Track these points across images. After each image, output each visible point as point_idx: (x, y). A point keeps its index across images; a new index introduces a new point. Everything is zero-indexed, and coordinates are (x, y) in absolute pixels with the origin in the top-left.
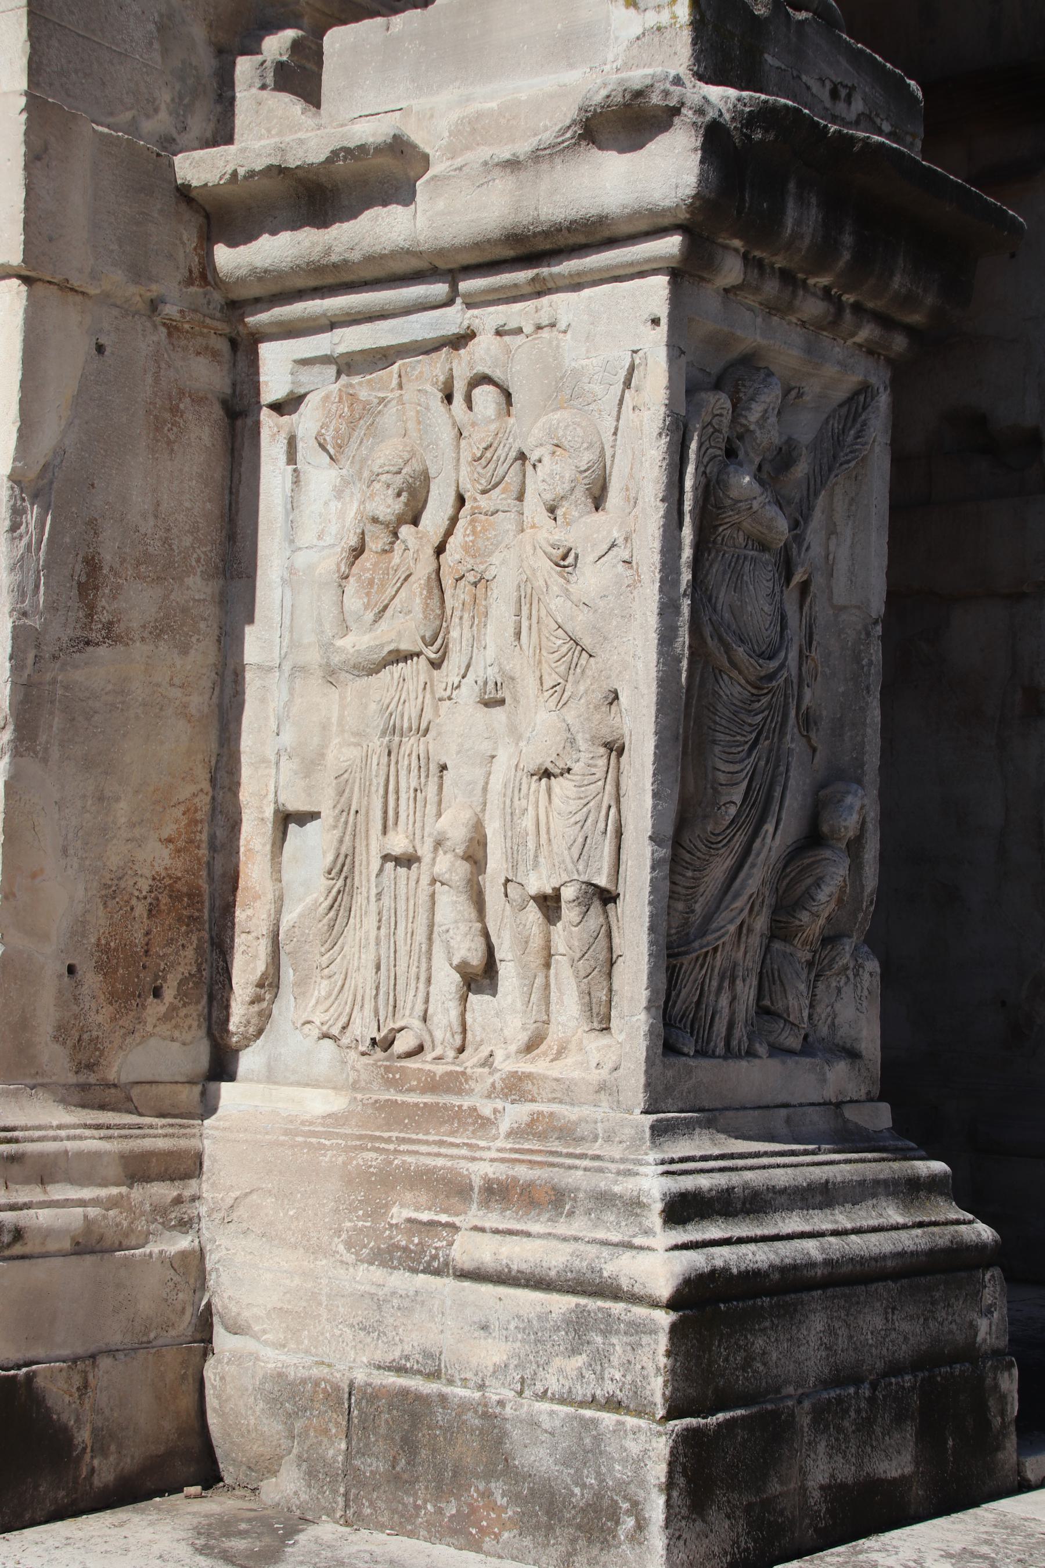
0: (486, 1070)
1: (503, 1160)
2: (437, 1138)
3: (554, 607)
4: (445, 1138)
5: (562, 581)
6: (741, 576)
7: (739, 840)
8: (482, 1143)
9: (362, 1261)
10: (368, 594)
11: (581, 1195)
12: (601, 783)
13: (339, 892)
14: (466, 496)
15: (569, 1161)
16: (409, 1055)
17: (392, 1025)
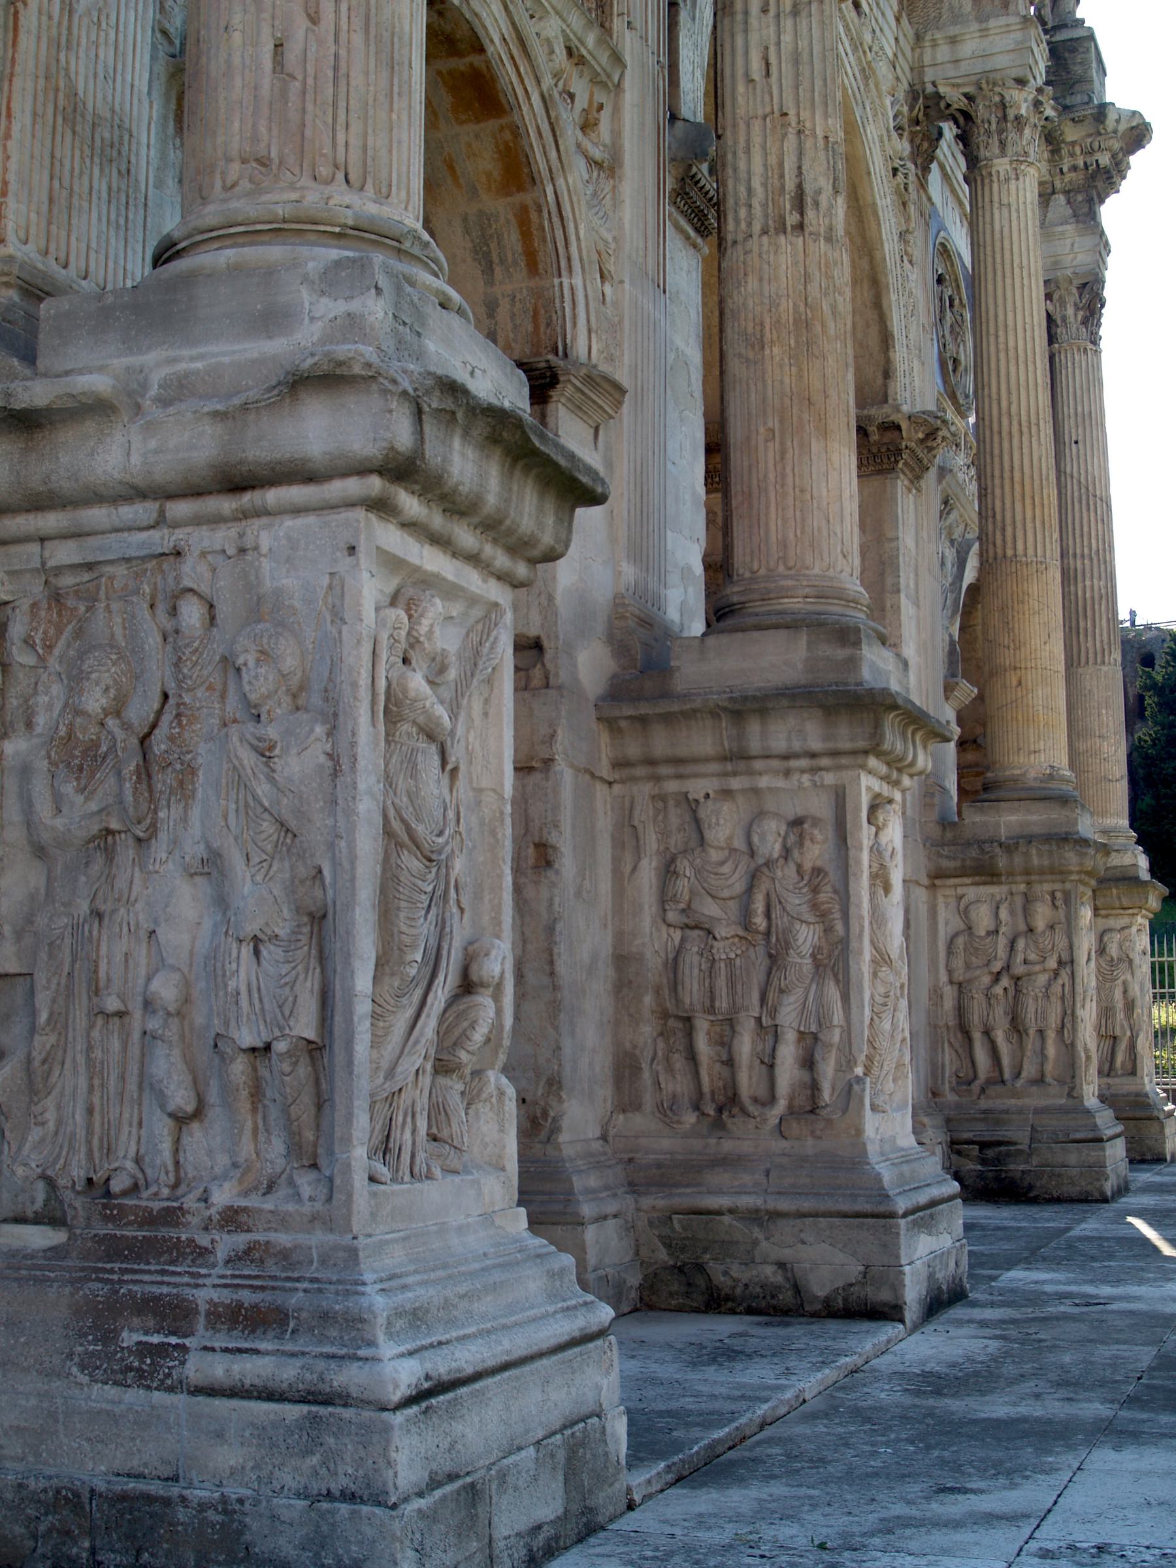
0: (203, 1205)
1: (225, 1286)
2: (159, 1268)
3: (260, 793)
5: (266, 770)
6: (415, 765)
7: (419, 993)
8: (203, 1271)
9: (96, 1381)
10: (78, 779)
11: (304, 1315)
14: (170, 693)
15: (288, 1285)
16: (125, 1193)
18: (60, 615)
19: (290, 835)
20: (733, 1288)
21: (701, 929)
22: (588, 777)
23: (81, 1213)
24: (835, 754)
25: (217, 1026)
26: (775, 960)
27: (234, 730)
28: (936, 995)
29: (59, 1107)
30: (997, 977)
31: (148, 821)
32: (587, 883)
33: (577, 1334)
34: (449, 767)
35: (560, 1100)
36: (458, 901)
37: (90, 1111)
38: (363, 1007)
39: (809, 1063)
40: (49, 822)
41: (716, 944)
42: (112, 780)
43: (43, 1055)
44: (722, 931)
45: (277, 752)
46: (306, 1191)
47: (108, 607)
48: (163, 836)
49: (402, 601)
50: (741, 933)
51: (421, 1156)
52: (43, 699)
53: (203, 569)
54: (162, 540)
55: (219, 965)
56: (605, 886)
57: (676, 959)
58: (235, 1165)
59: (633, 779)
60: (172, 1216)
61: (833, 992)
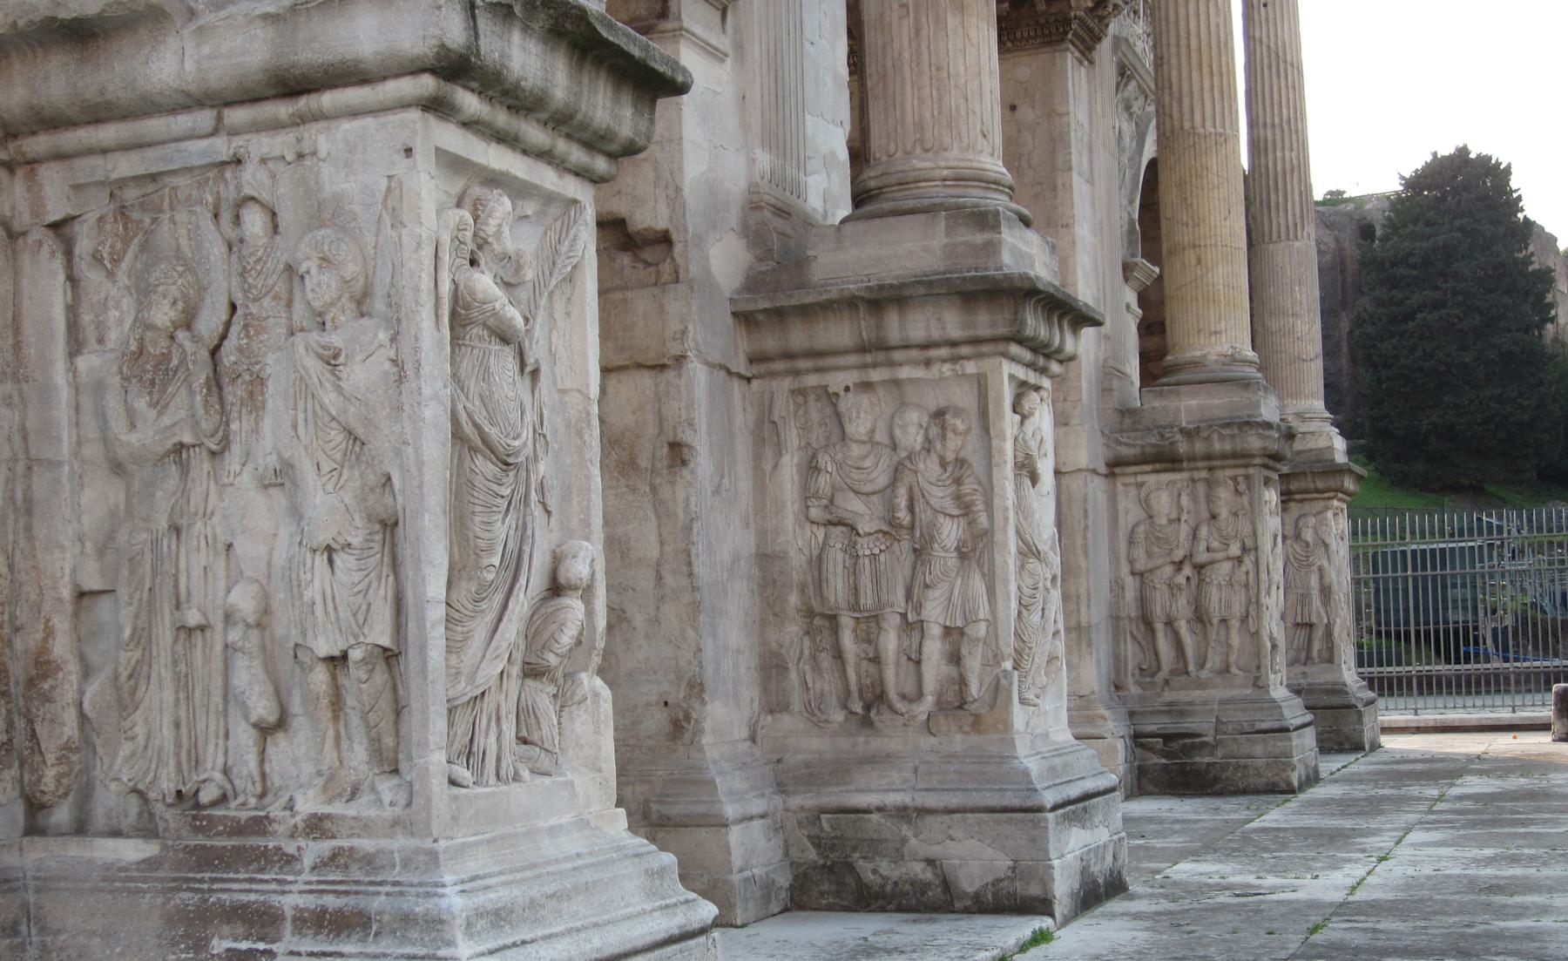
0: (288, 813)
1: (311, 892)
2: (247, 876)
3: (327, 401)
4: (254, 876)
5: (332, 378)
7: (498, 598)
8: (290, 878)
10: (150, 393)
11: (386, 918)
12: (379, 556)
13: (138, 662)
14: (238, 303)
15: (372, 888)
16: (214, 804)
17: (195, 778)
18: (126, 228)
19: (358, 443)
20: (883, 886)
21: (845, 525)
22: (723, 373)
23: (172, 825)
24: (975, 341)
25: (295, 637)
26: (920, 553)
27: (299, 337)
28: (1117, 586)
29: (146, 721)
30: (1179, 566)
31: (220, 434)
32: (726, 481)
33: (676, 932)
34: (528, 369)
35: (703, 702)
36: (544, 504)
37: (177, 725)
38: (437, 613)
39: (955, 659)
40: (124, 438)
41: (860, 540)
42: (183, 392)
43: (130, 669)
44: (864, 527)
45: (342, 359)
46: (387, 797)
47: (173, 221)
48: (236, 448)
49: (468, 201)
50: (885, 528)
51: (507, 760)
52: (114, 314)
53: (263, 175)
54: (222, 147)
55: (294, 576)
56: (745, 484)
57: (820, 556)
58: (319, 773)
59: (773, 374)
60: (259, 825)
61: (978, 585)
